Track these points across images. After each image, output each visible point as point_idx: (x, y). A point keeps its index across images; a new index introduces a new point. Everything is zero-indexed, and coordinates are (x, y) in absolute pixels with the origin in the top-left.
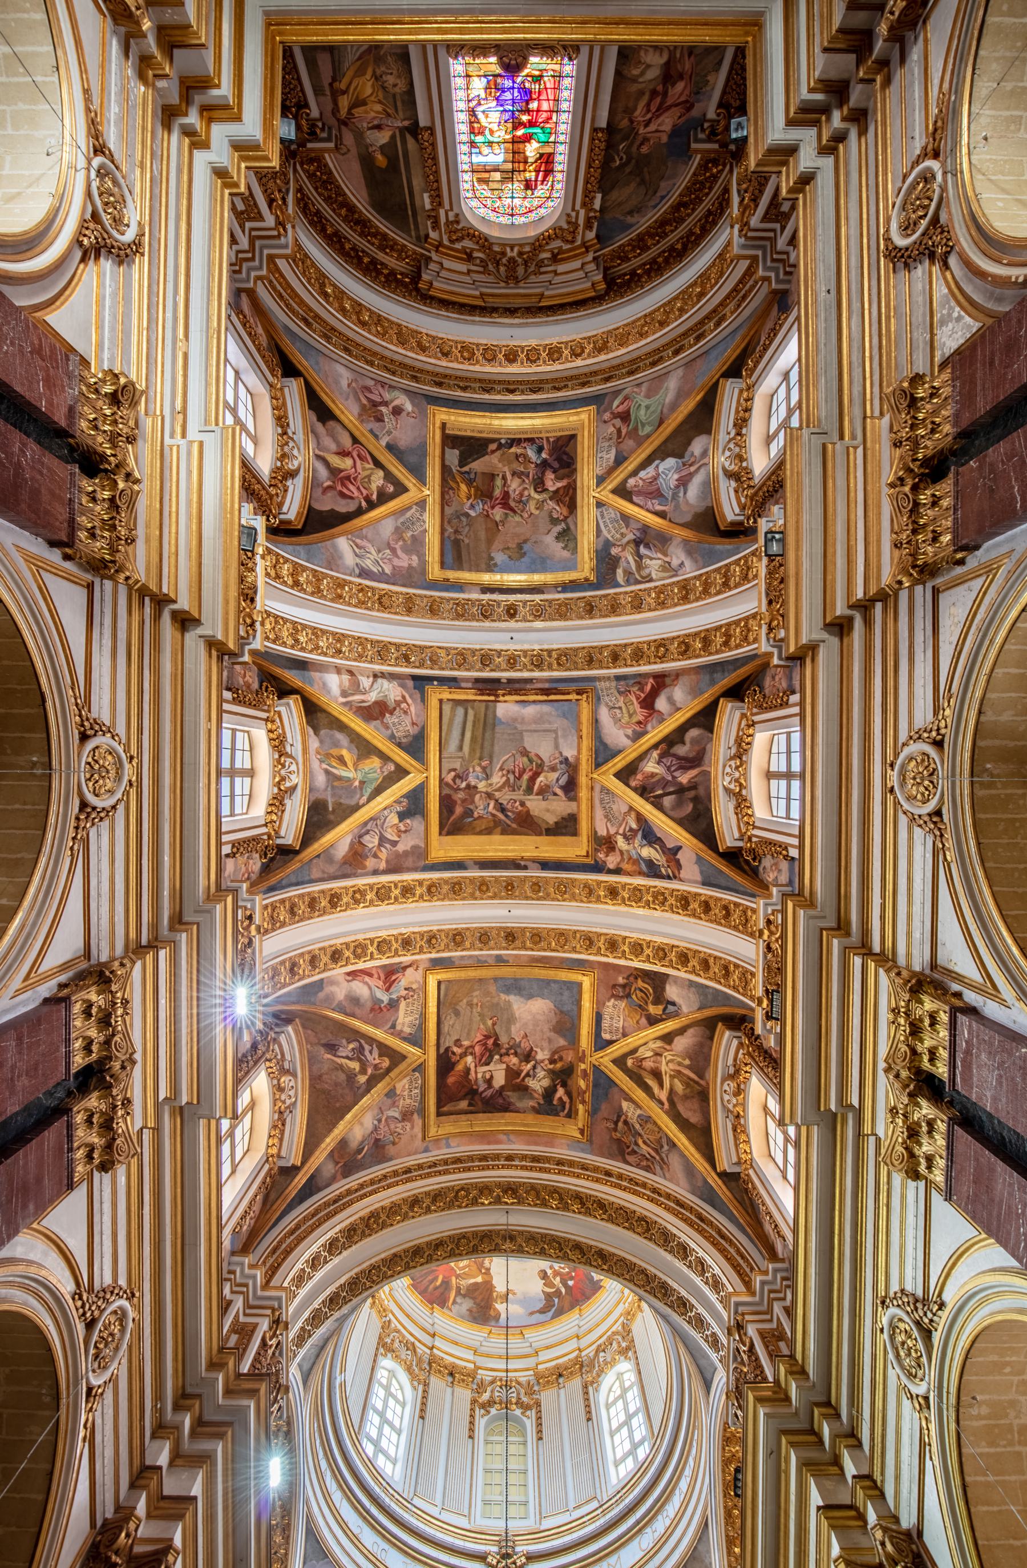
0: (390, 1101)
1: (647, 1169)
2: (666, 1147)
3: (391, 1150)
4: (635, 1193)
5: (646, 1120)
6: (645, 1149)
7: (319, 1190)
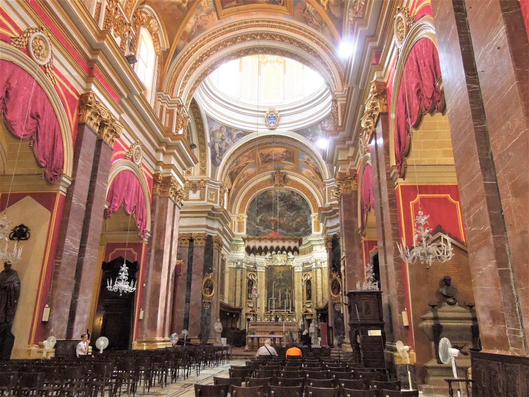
0: (199, 10)
1: (316, 29)
2: (324, 25)
3: (205, 27)
4: (310, 39)
5: (316, 13)
6: (315, 22)
7: (180, 51)
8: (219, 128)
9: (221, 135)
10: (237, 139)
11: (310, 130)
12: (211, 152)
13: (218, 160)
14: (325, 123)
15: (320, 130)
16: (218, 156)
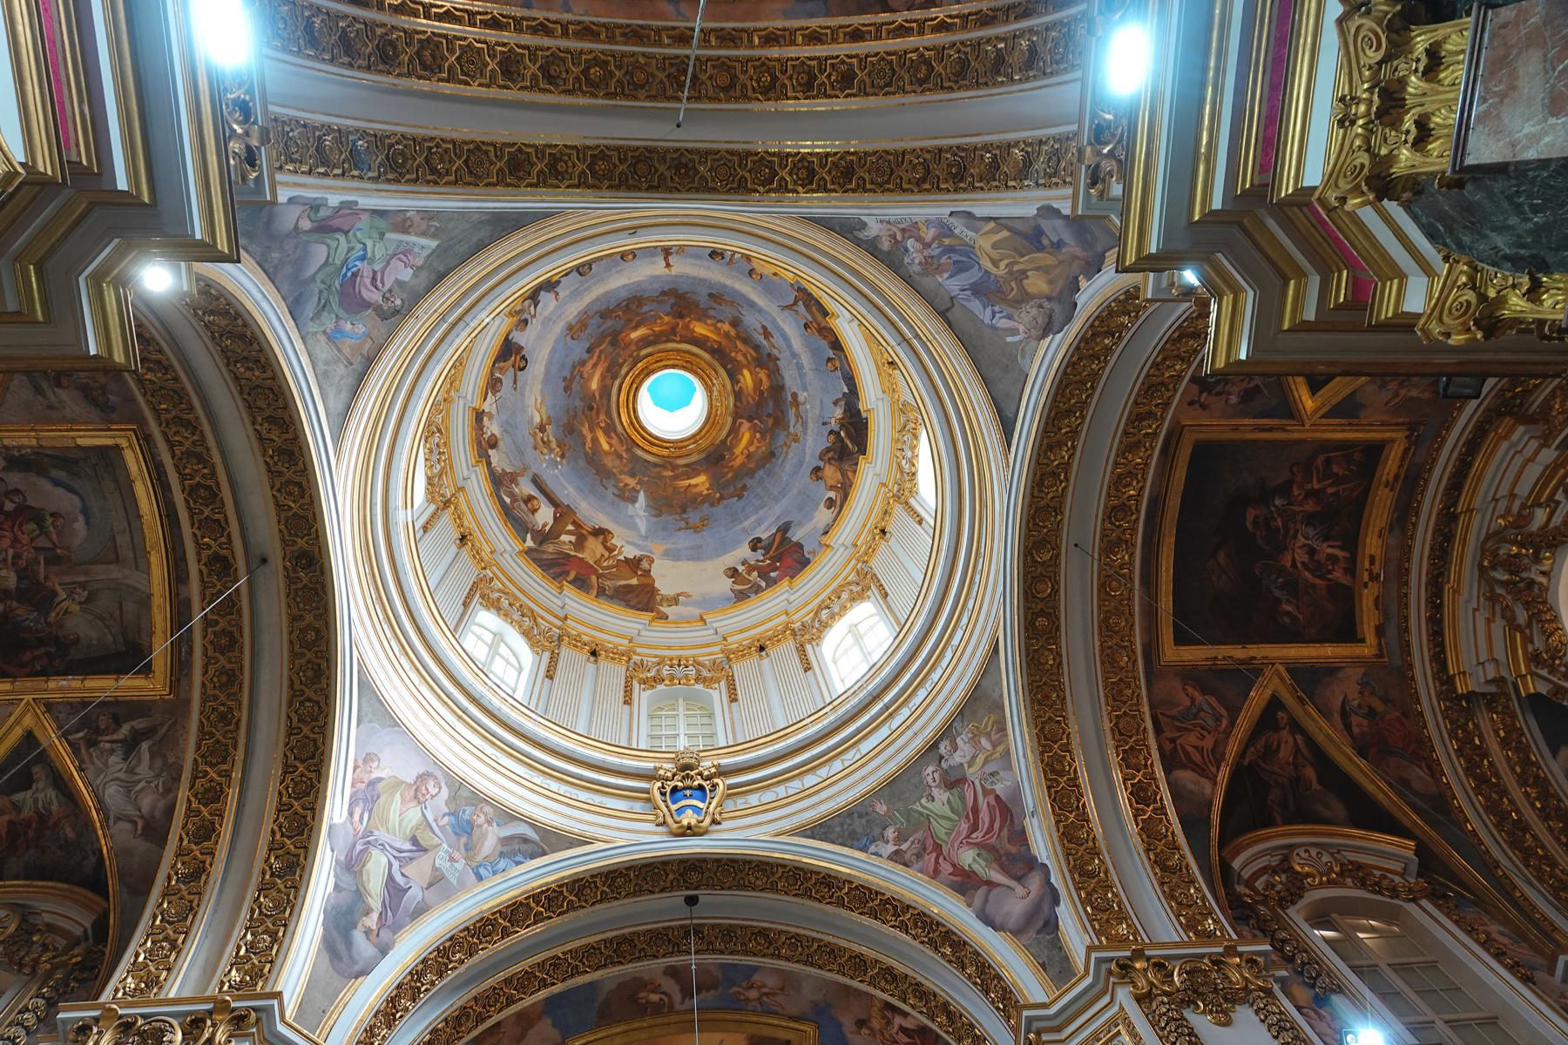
8: (410, 779)
9: (414, 815)
10: (502, 864)
11: (881, 808)
12: (337, 887)
13: (363, 947)
14: (955, 749)
15: (935, 792)
16: (372, 921)
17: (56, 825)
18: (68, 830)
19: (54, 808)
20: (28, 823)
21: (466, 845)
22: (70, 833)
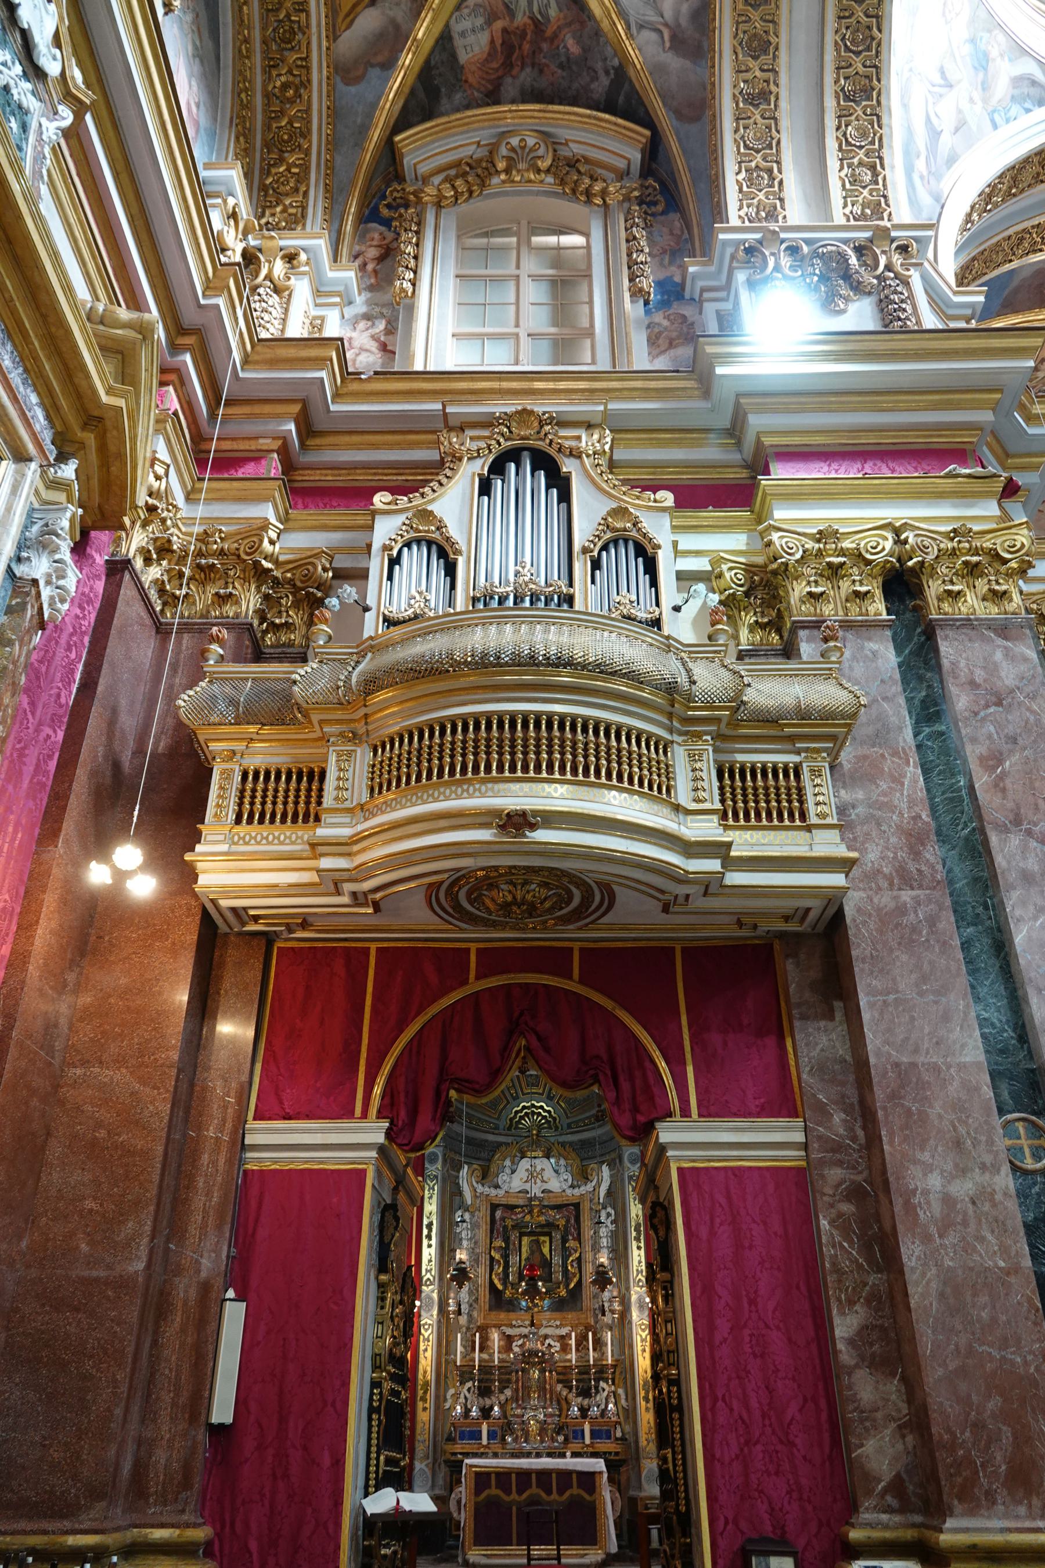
10: (1015, 109)
17: (555, 36)
18: (570, 42)
19: (553, 12)
20: (523, 35)
21: (983, 83)
22: (573, 46)
